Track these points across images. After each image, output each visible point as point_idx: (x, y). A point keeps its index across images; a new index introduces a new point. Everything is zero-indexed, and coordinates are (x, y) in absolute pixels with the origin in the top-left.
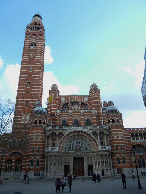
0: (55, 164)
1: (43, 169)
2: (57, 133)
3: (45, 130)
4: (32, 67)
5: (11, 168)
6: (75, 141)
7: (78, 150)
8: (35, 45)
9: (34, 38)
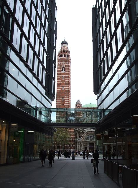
0: (80, 146)
1: (75, 148)
2: (81, 132)
3: (75, 130)
4: (64, 87)
5: (60, 147)
6: (90, 136)
7: (91, 140)
8: (65, 70)
9: (64, 64)
